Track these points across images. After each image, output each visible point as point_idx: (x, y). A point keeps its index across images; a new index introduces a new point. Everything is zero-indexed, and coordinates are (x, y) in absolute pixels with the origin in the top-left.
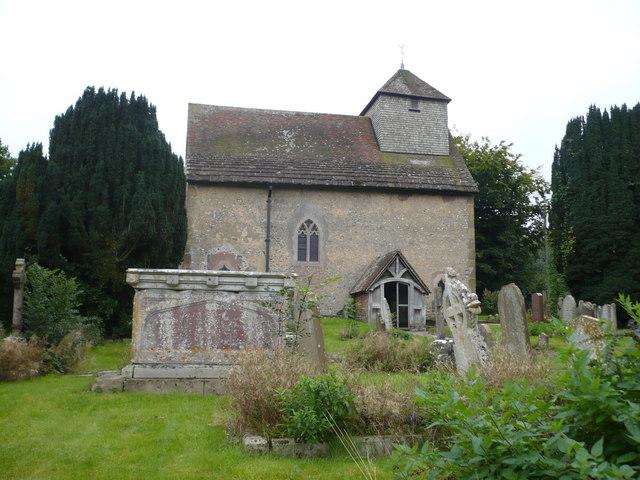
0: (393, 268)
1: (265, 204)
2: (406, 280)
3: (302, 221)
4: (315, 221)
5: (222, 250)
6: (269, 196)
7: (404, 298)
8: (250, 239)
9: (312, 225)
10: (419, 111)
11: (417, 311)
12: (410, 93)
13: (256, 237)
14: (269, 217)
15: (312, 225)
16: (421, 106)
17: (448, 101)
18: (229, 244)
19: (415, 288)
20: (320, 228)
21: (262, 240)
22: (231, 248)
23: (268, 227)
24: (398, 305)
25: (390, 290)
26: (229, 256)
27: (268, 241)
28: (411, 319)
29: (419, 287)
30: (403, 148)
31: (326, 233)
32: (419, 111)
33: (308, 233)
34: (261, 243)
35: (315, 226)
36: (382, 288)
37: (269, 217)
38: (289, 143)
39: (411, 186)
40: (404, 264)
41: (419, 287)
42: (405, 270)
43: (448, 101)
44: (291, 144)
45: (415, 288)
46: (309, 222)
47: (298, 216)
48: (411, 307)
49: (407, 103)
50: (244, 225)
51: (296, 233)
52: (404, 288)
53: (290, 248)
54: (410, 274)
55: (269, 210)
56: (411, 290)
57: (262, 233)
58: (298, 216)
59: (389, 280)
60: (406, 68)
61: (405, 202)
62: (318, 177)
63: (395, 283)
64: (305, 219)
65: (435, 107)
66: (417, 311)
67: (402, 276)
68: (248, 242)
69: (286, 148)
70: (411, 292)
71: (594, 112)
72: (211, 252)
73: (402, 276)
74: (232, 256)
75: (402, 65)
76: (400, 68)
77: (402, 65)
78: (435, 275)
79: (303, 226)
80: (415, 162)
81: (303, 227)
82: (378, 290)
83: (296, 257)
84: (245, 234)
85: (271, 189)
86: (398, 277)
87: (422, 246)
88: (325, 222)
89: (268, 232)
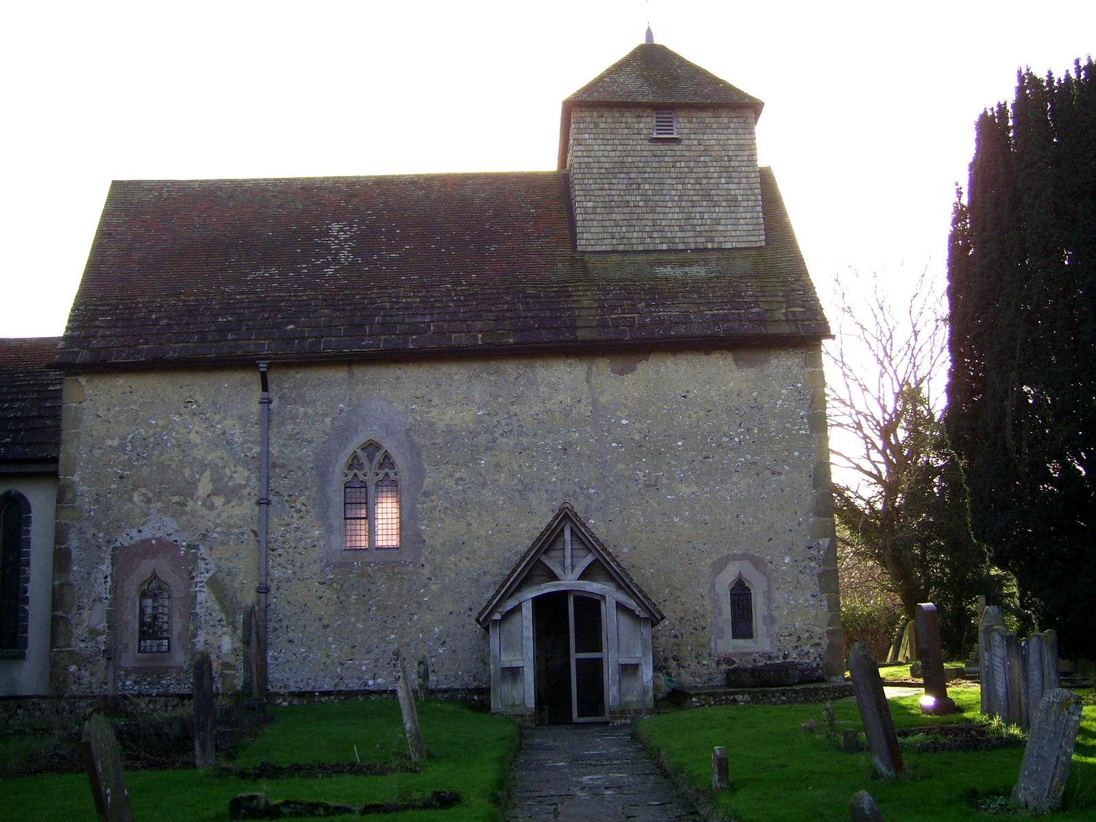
2: (593, 587)
3: (355, 444)
4: (388, 445)
5: (148, 533)
6: (265, 388)
7: (591, 635)
8: (218, 501)
9: (379, 456)
10: (677, 141)
11: (629, 670)
12: (649, 98)
13: (232, 493)
15: (379, 456)
16: (682, 125)
18: (168, 520)
19: (620, 607)
22: (171, 524)
23: (266, 466)
24: (575, 656)
27: (264, 502)
28: (612, 694)
29: (632, 604)
30: (636, 238)
31: (418, 472)
32: (677, 141)
34: (245, 509)
35: (387, 456)
36: (527, 611)
40: (585, 540)
41: (632, 604)
42: (589, 559)
44: (343, 255)
45: (620, 607)
46: (371, 447)
48: (612, 659)
49: (647, 124)
50: (204, 466)
52: (590, 607)
54: (600, 568)
55: (267, 420)
56: (609, 612)
58: (342, 434)
59: (548, 588)
60: (658, 40)
61: (629, 378)
63: (562, 595)
66: (629, 670)
67: (584, 575)
68: (212, 507)
69: (327, 265)
71: (1029, 85)
72: (123, 540)
73: (584, 575)
74: (175, 545)
75: (649, 34)
76: (643, 41)
77: (649, 34)
78: (720, 566)
79: (355, 457)
80: (662, 271)
81: (354, 463)
82: (515, 619)
84: (204, 487)
86: (569, 581)
87: (684, 490)
88: (413, 445)
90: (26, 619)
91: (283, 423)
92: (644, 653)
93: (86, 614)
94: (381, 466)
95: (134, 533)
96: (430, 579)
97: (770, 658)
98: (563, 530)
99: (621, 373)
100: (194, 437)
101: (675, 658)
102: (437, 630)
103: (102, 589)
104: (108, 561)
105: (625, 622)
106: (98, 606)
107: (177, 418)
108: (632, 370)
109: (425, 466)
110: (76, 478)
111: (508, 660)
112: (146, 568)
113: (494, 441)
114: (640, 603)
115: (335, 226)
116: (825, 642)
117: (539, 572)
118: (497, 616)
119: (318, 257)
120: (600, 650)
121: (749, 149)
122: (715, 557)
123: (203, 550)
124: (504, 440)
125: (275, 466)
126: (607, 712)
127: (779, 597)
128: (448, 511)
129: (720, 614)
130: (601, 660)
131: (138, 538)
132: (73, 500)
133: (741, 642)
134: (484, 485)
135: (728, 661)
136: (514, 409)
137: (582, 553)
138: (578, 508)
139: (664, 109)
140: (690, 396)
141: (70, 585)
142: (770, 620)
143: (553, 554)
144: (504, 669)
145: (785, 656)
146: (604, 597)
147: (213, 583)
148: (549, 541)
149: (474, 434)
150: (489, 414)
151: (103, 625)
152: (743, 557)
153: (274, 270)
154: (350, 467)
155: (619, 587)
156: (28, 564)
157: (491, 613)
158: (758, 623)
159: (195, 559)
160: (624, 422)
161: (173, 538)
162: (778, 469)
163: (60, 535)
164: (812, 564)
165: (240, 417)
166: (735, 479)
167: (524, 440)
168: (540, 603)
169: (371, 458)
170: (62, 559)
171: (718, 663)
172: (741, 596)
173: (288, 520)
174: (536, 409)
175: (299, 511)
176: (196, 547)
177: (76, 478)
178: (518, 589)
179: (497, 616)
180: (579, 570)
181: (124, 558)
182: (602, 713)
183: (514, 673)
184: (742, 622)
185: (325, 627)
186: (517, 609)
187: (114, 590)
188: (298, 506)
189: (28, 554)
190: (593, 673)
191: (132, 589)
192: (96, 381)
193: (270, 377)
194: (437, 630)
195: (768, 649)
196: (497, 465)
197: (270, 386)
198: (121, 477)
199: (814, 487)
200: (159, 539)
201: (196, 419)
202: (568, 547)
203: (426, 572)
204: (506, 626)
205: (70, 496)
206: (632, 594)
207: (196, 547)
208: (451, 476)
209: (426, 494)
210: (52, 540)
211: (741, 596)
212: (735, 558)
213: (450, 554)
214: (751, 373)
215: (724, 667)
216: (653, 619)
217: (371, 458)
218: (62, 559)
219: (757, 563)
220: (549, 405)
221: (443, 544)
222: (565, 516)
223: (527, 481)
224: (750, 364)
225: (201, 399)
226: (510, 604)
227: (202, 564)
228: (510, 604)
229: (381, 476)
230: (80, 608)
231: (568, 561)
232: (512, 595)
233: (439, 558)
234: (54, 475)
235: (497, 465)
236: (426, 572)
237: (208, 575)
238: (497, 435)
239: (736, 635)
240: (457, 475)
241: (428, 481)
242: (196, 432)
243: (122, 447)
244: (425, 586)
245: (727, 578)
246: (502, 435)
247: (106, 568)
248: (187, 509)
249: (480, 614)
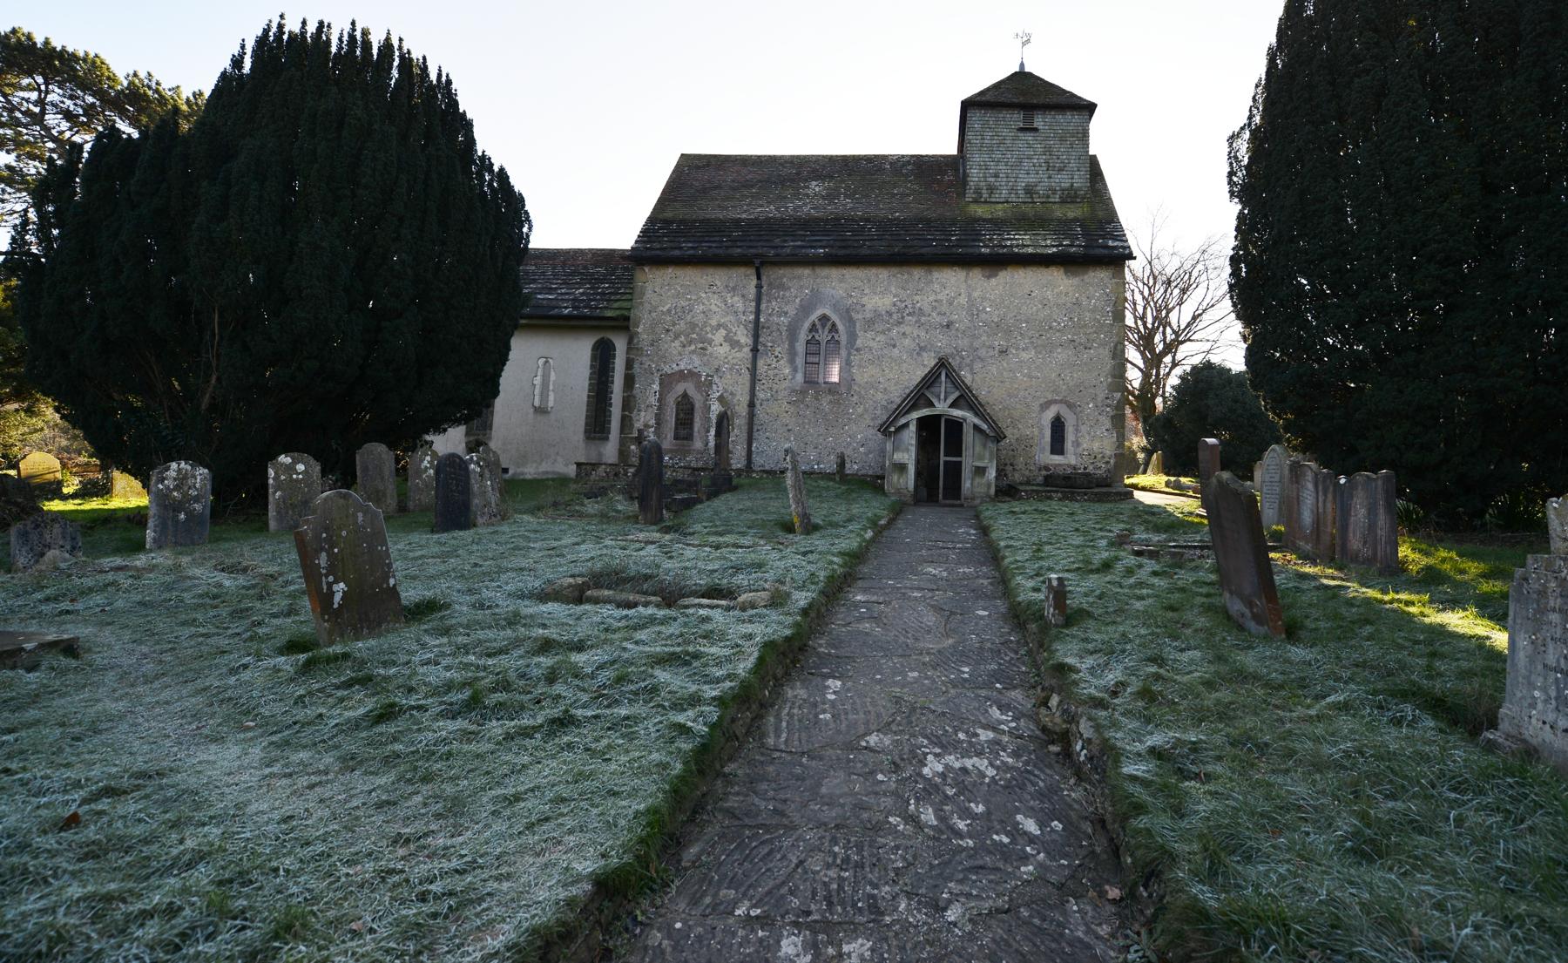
1: (751, 291)
2: (957, 413)
3: (814, 317)
4: (834, 318)
6: (759, 278)
7: (955, 446)
9: (829, 325)
11: (980, 471)
14: (758, 312)
15: (829, 325)
16: (1039, 121)
17: (1089, 108)
19: (976, 427)
20: (840, 327)
21: (747, 350)
22: (697, 361)
23: (757, 330)
24: (943, 458)
25: (928, 426)
26: (692, 375)
27: (755, 350)
28: (966, 484)
29: (984, 427)
31: (852, 336)
32: (1036, 130)
33: (823, 336)
35: (834, 325)
36: (913, 427)
37: (758, 312)
38: (811, 200)
40: (955, 381)
42: (957, 394)
43: (1089, 108)
47: (806, 309)
48: (968, 461)
49: (1016, 118)
51: (803, 336)
52: (955, 426)
53: (792, 361)
54: (966, 399)
57: (744, 338)
58: (806, 309)
59: (925, 412)
61: (993, 281)
62: (838, 244)
63: (938, 417)
64: (819, 312)
65: (1069, 120)
66: (980, 471)
67: (952, 406)
70: (968, 436)
72: (667, 369)
73: (952, 406)
74: (699, 375)
75: (1022, 65)
76: (1018, 70)
77: (1022, 65)
78: (1046, 405)
79: (814, 325)
81: (813, 328)
83: (800, 377)
85: (758, 263)
86: (941, 407)
87: (1025, 355)
89: (756, 336)
90: (610, 416)
91: (769, 301)
92: (991, 461)
93: (643, 414)
94: (830, 331)
95: (674, 366)
97: (1075, 469)
98: (940, 374)
100: (713, 308)
101: (1011, 465)
103: (653, 400)
104: (657, 383)
105: (979, 439)
106: (650, 409)
107: (704, 295)
108: (996, 275)
110: (639, 330)
111: (899, 457)
112: (680, 388)
113: (903, 317)
114: (990, 426)
115: (814, 183)
116: (1112, 461)
117: (922, 402)
118: (892, 429)
119: (800, 200)
120: (961, 456)
121: (1084, 136)
122: (1042, 401)
123: (716, 379)
125: (763, 327)
126: (963, 497)
127: (1084, 429)
129: (1043, 438)
130: (961, 462)
131: (676, 368)
132: (638, 343)
133: (1057, 459)
134: (894, 346)
135: (1046, 468)
136: (918, 298)
137: (953, 390)
138: (954, 363)
139: (1029, 108)
140: (1033, 294)
141: (635, 397)
142: (1077, 444)
143: (932, 389)
145: (1085, 468)
146: (965, 420)
147: (721, 399)
148: (930, 380)
149: (890, 314)
151: (652, 422)
152: (1061, 402)
153: (772, 207)
154: (811, 331)
155: (976, 414)
156: (612, 382)
157: (888, 427)
158: (1069, 445)
159: (711, 383)
160: (988, 309)
161: (698, 370)
162: (1089, 345)
163: (629, 364)
164: (1108, 409)
165: (743, 296)
166: (1059, 350)
167: (923, 319)
169: (824, 326)
170: (629, 381)
171: (1040, 470)
172: (1058, 426)
173: (769, 362)
174: (931, 299)
175: (777, 357)
176: (712, 376)
177: (639, 330)
178: (908, 412)
179: (892, 429)
180: (950, 401)
181: (667, 381)
182: (958, 498)
183: (902, 468)
184: (1058, 445)
185: (789, 430)
186: (906, 425)
187: (660, 400)
188: (777, 354)
189: (613, 376)
190: (955, 471)
191: (671, 400)
192: (654, 270)
193: (762, 271)
195: (1073, 462)
196: (904, 334)
197: (764, 278)
198: (668, 330)
199: (1113, 359)
200: (689, 371)
201: (716, 296)
202: (943, 384)
204: (899, 436)
205: (635, 341)
206: (985, 421)
207: (712, 376)
208: (874, 339)
209: (858, 350)
210: (624, 368)
211: (1058, 426)
212: (1055, 402)
214: (1075, 281)
215: (1044, 473)
216: (999, 437)
217: (824, 326)
218: (629, 381)
219: (1070, 406)
220: (939, 297)
222: (942, 363)
223: (922, 344)
224: (1075, 274)
225: (719, 284)
226: (903, 421)
227: (714, 387)
228: (903, 421)
229: (829, 338)
230: (639, 411)
231: (942, 397)
234: (627, 328)
235: (904, 334)
236: (855, 399)
237: (718, 394)
239: (1053, 452)
241: (859, 343)
242: (715, 303)
243: (669, 311)
245: (1050, 414)
247: (656, 387)
248: (708, 352)
249: (882, 426)
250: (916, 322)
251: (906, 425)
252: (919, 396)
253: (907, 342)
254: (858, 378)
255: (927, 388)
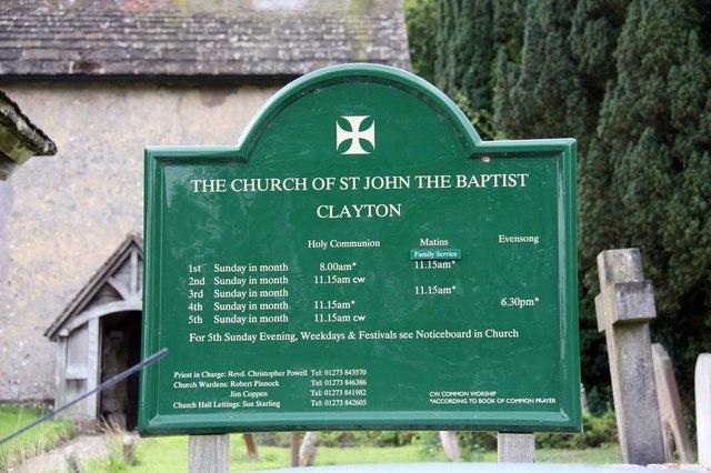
0: (122, 277)
36: (94, 331)
39: (230, 69)
59: (112, 307)
61: (219, 110)
82: (82, 336)
96: (16, 295)
98: (129, 256)
99: (211, 105)
102: (21, 344)
108: (221, 102)
109: (15, 188)
111: (74, 372)
113: (85, 166)
117: (106, 292)
118: (64, 332)
124: (94, 166)
128: (38, 233)
134: (73, 208)
136: (107, 136)
143: (118, 276)
144: (68, 381)
150: (81, 140)
157: (59, 328)
167: (115, 168)
168: (108, 323)
174: (128, 136)
178: (86, 308)
183: (78, 383)
186: (84, 326)
194: (21, 344)
203: (13, 289)
209: (16, 215)
213: (37, 272)
221: (31, 263)
226: (77, 322)
228: (77, 322)
232: (80, 313)
233: (26, 277)
235: (88, 190)
236: (13, 289)
238: (87, 161)
240: (47, 197)
244: (12, 302)
246: (93, 161)
250: (106, 171)
251: (84, 326)
252: (101, 289)
253: (92, 201)
254: (18, 258)
255: (113, 275)
